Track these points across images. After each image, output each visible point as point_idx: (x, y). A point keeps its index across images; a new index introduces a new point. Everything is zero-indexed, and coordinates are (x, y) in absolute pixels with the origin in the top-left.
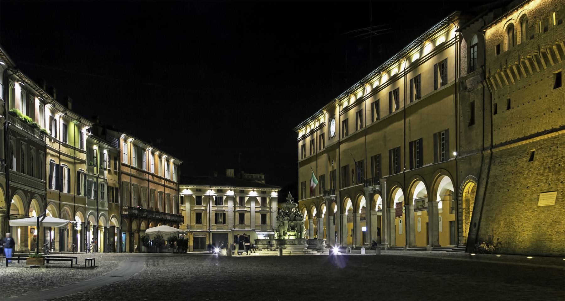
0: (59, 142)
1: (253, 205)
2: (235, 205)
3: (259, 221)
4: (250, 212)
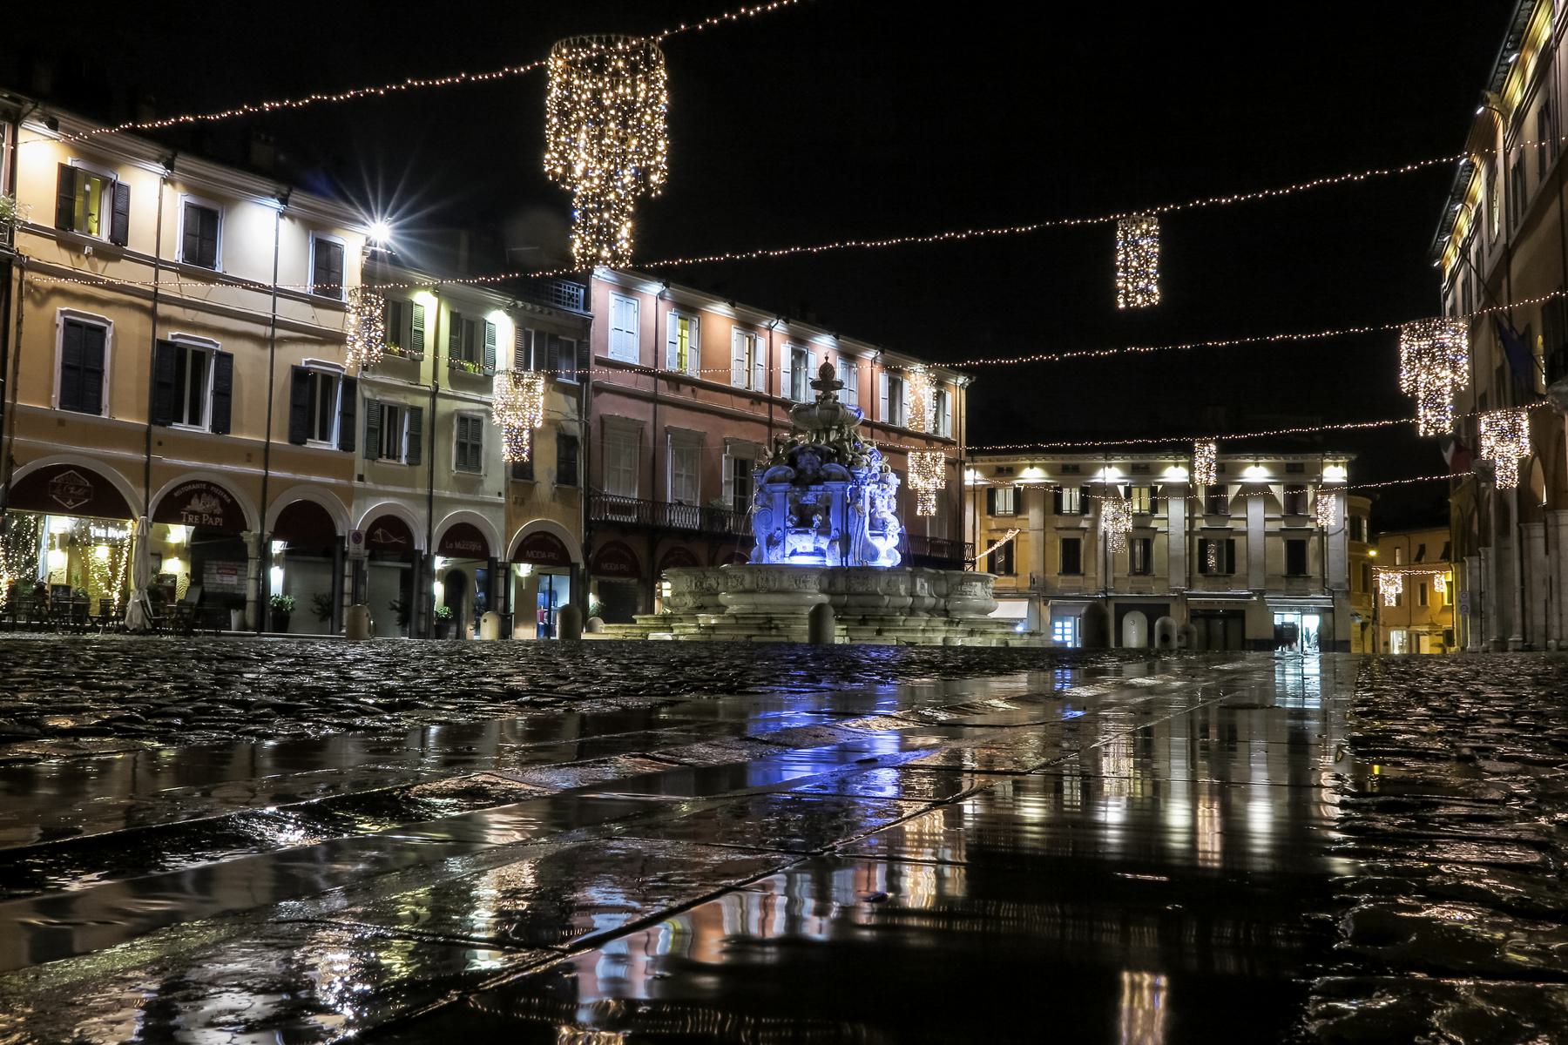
0: (157, 263)
1: (1256, 512)
2: (1192, 512)
3: (1281, 565)
4: (1245, 533)
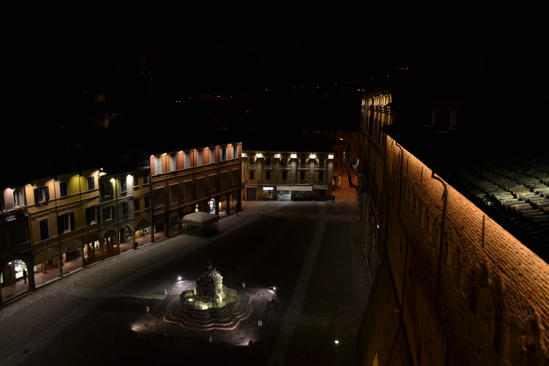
1: (312, 165)
2: (297, 165)
